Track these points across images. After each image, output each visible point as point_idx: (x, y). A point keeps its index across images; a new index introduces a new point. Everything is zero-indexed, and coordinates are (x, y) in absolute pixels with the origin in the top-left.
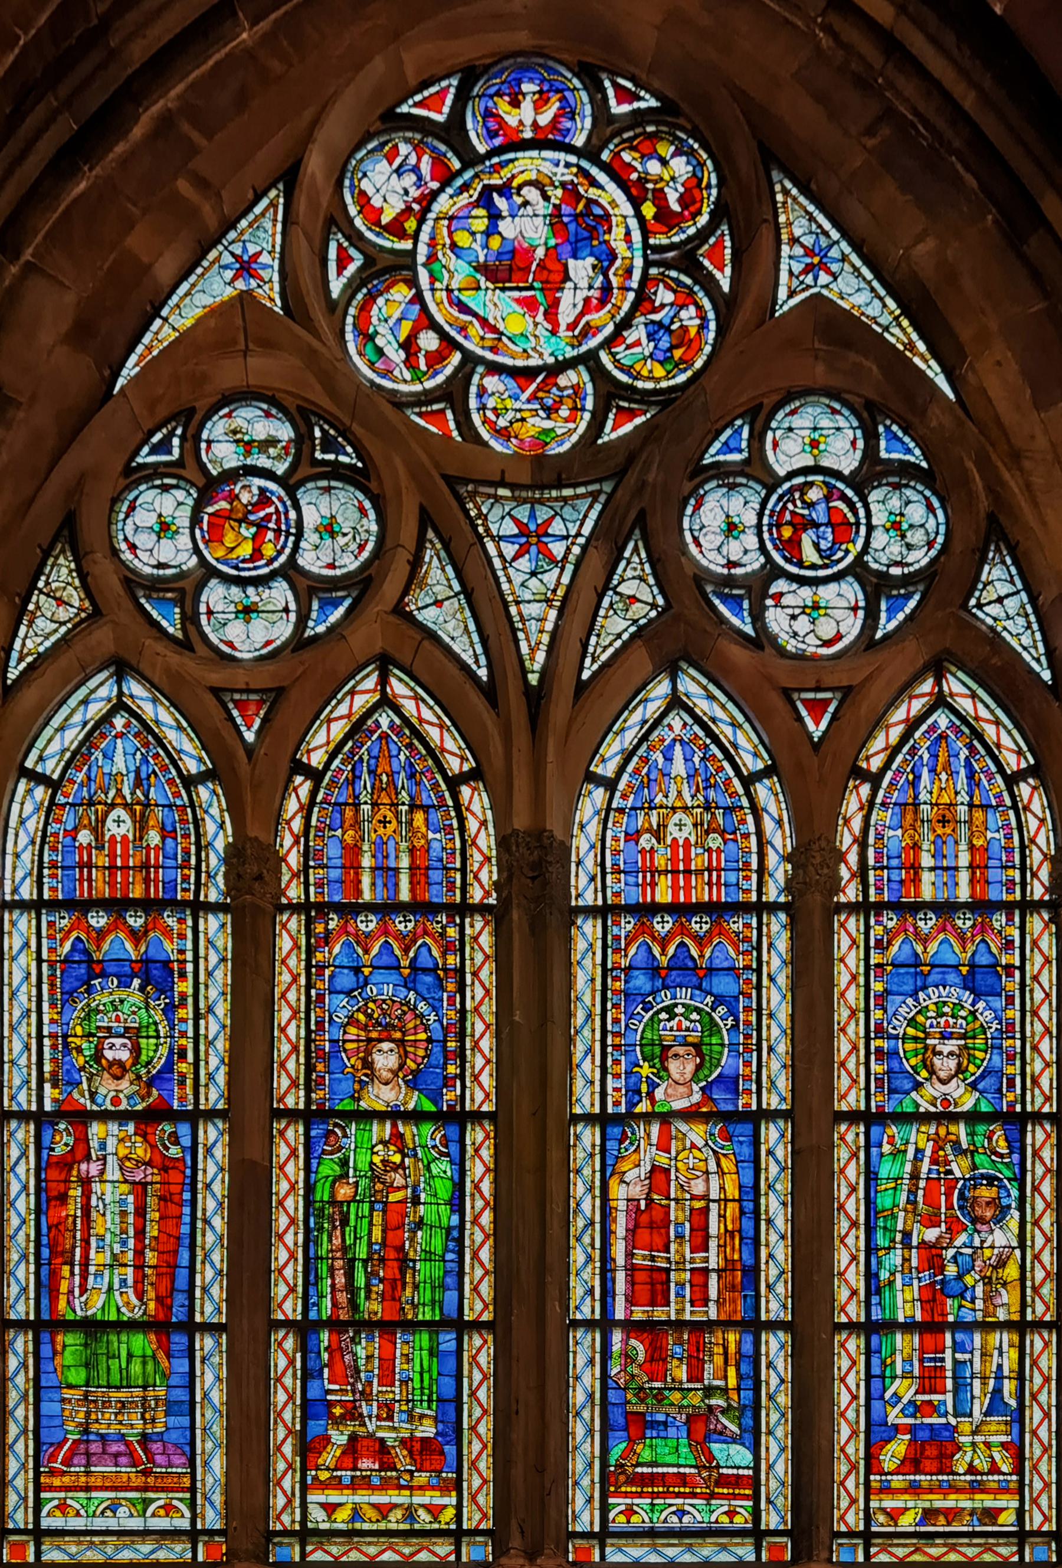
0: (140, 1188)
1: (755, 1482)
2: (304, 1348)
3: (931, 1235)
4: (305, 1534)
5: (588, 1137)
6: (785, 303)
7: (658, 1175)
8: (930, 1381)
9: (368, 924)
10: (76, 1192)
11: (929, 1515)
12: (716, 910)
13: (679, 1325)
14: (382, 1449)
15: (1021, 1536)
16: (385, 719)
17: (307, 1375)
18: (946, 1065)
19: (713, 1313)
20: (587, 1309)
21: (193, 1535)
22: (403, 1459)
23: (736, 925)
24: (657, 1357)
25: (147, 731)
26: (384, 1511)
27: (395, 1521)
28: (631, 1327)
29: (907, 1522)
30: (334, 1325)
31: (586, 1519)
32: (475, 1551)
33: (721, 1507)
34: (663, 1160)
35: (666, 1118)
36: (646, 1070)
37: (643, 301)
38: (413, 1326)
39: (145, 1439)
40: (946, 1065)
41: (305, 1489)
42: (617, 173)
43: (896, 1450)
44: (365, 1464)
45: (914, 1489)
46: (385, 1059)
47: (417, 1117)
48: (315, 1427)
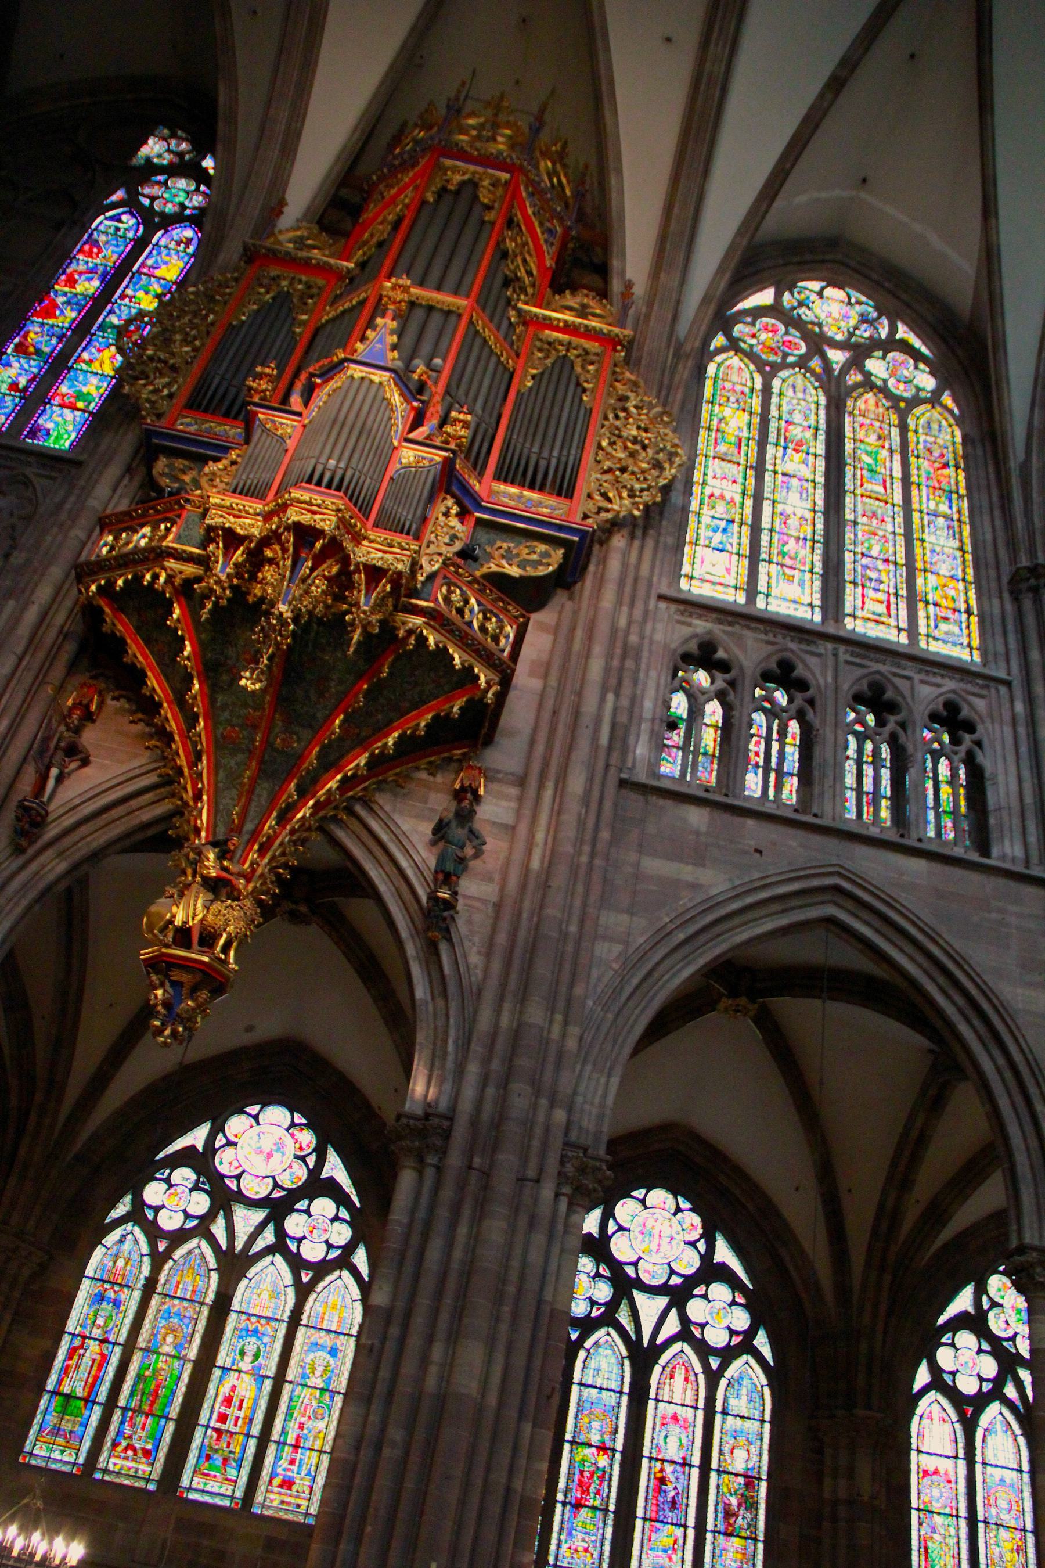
0: (94, 1360)
1: (235, 1482)
2: (123, 1415)
3: (303, 1420)
4: (105, 1471)
5: (217, 1373)
6: (324, 1175)
7: (234, 1388)
8: (292, 1462)
9: (176, 1302)
10: (76, 1357)
11: (283, 1502)
12: (268, 1319)
13: (228, 1431)
14: (135, 1450)
15: (307, 1514)
16: (197, 1251)
17: (122, 1423)
18: (318, 1373)
19: (237, 1429)
20: (203, 1420)
21: (74, 1464)
22: (140, 1454)
23: (273, 1323)
24: (219, 1439)
25: (136, 1241)
26: (130, 1468)
27: (132, 1472)
28: (214, 1429)
29: (275, 1504)
30: (134, 1411)
31: (185, 1482)
32: (152, 1487)
33: (225, 1487)
34: (236, 1383)
35: (240, 1372)
36: (238, 1357)
37: (290, 1167)
38: (154, 1415)
39: (71, 1432)
40: (318, 1373)
41: (110, 1456)
42: (293, 1135)
43: (277, 1481)
44: (130, 1453)
45: (280, 1493)
46: (170, 1339)
47: (173, 1357)
48: (119, 1439)
